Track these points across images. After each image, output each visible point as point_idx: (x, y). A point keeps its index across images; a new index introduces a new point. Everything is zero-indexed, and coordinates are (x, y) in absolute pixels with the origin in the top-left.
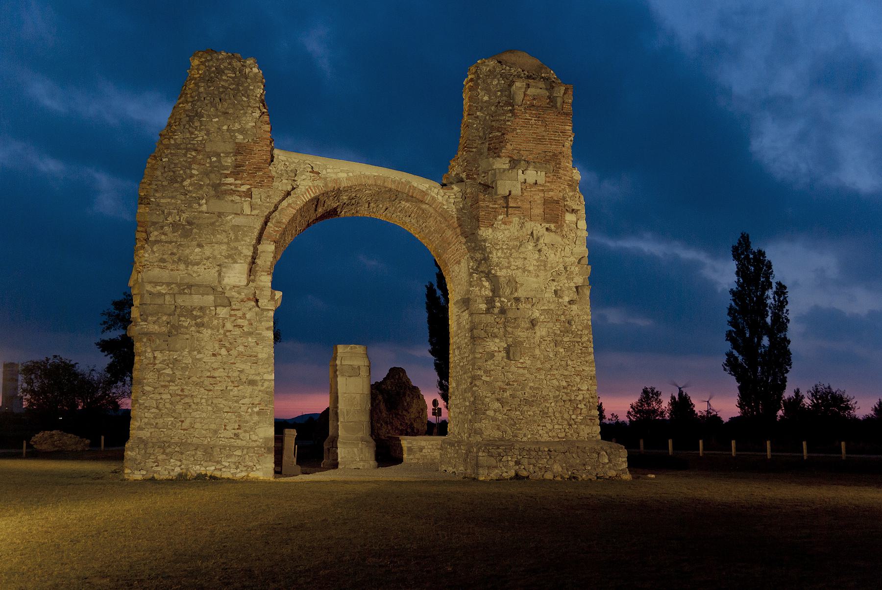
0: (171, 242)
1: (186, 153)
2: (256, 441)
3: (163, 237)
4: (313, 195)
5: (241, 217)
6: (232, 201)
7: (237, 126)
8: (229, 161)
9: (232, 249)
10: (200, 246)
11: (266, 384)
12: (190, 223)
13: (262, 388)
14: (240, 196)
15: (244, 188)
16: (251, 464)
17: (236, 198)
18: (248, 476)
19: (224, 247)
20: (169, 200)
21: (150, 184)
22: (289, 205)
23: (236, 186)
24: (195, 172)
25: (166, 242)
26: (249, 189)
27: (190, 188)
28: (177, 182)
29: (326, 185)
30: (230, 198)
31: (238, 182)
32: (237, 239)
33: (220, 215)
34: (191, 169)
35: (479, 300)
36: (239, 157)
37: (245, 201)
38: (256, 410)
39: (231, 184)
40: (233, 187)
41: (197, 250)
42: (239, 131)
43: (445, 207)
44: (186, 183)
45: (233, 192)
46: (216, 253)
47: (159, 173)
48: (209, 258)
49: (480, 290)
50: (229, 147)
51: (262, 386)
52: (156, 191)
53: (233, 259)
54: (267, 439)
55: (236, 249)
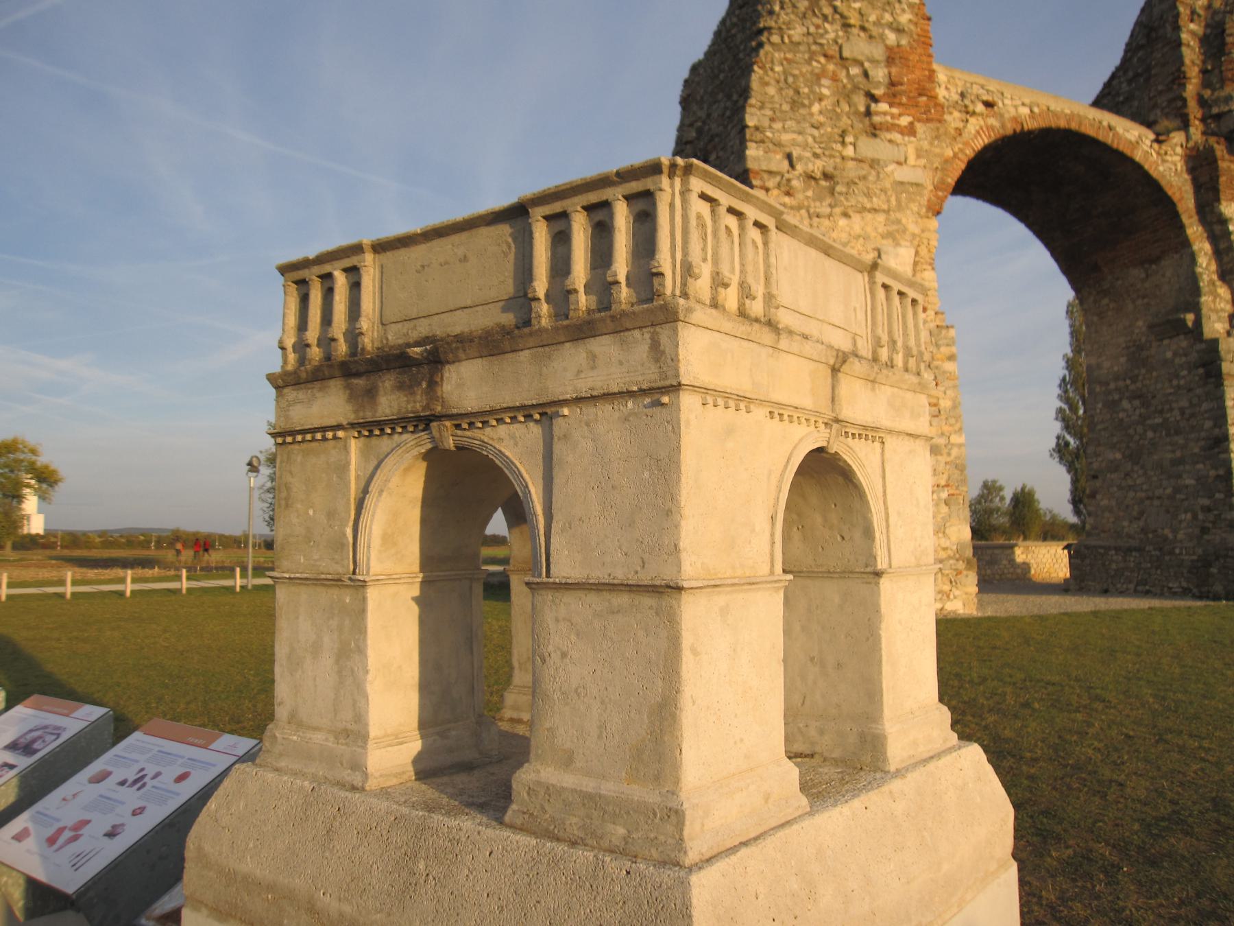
0: (799, 208)
1: (811, 59)
2: (945, 549)
3: (787, 200)
4: (986, 141)
5: (905, 167)
6: (890, 141)
7: (888, 17)
8: (879, 74)
9: (893, 223)
10: (846, 215)
11: (955, 452)
12: (826, 176)
13: (948, 459)
14: (902, 133)
15: (904, 121)
16: (946, 588)
17: (896, 136)
18: (942, 609)
19: (881, 218)
20: (794, 136)
21: (761, 108)
22: (955, 155)
23: (893, 116)
24: (825, 91)
25: (792, 208)
26: (911, 123)
27: (822, 119)
28: (803, 105)
29: (1003, 126)
30: (889, 136)
31: (895, 111)
32: (899, 207)
33: (874, 163)
34: (820, 86)
35: (1214, 317)
36: (894, 70)
37: (910, 142)
38: (944, 495)
39: (885, 114)
40: (888, 118)
41: (842, 222)
42: (890, 26)
43: (1161, 168)
44: (816, 108)
45: (891, 128)
46: (869, 229)
47: (771, 91)
48: (859, 236)
49: (1214, 301)
50: (878, 52)
51: (949, 454)
52: (772, 120)
53: (894, 239)
54: (961, 546)
55: (899, 222)
